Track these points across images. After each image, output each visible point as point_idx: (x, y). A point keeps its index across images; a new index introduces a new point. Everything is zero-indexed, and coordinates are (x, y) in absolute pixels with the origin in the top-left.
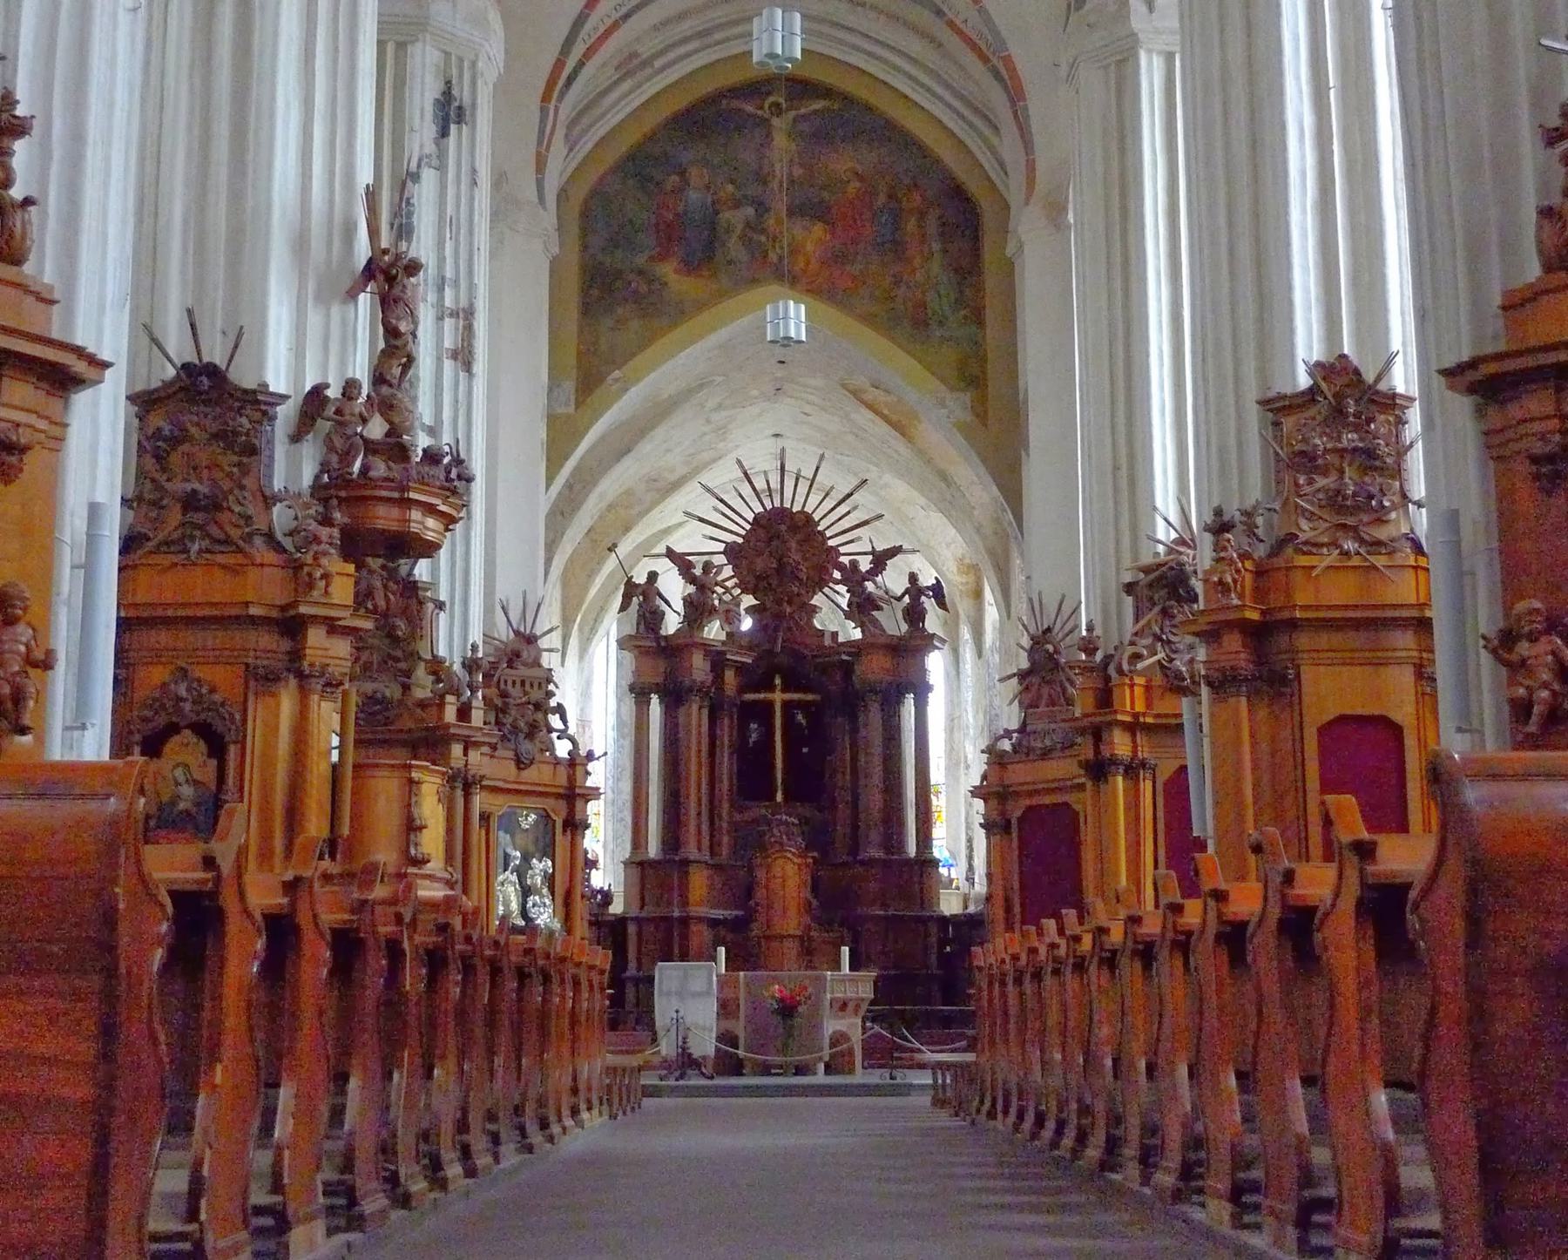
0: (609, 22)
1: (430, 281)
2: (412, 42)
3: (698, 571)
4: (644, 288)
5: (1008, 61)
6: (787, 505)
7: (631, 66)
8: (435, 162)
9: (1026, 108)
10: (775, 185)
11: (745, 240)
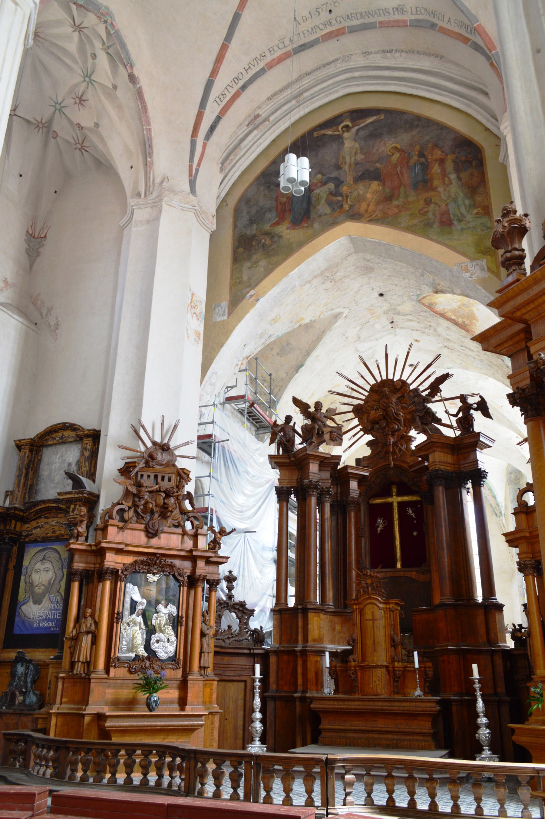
0: (233, 91)
3: (312, 410)
4: (268, 242)
6: (390, 377)
10: (346, 167)
11: (330, 203)
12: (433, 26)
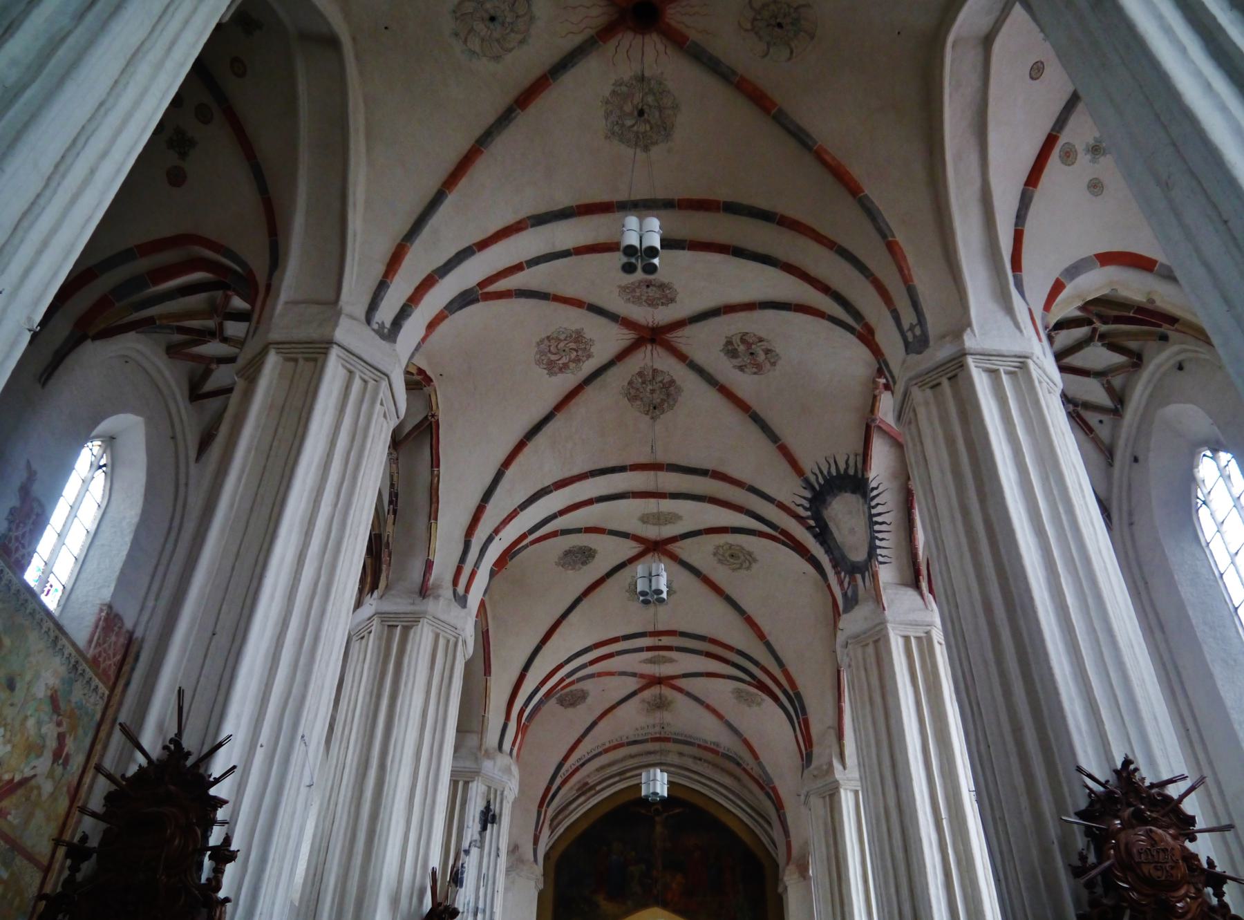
0: (574, 767)
1: (470, 910)
2: (472, 781)
5: (774, 789)
7: (585, 789)
8: (478, 844)
9: (784, 814)
12: (738, 764)
